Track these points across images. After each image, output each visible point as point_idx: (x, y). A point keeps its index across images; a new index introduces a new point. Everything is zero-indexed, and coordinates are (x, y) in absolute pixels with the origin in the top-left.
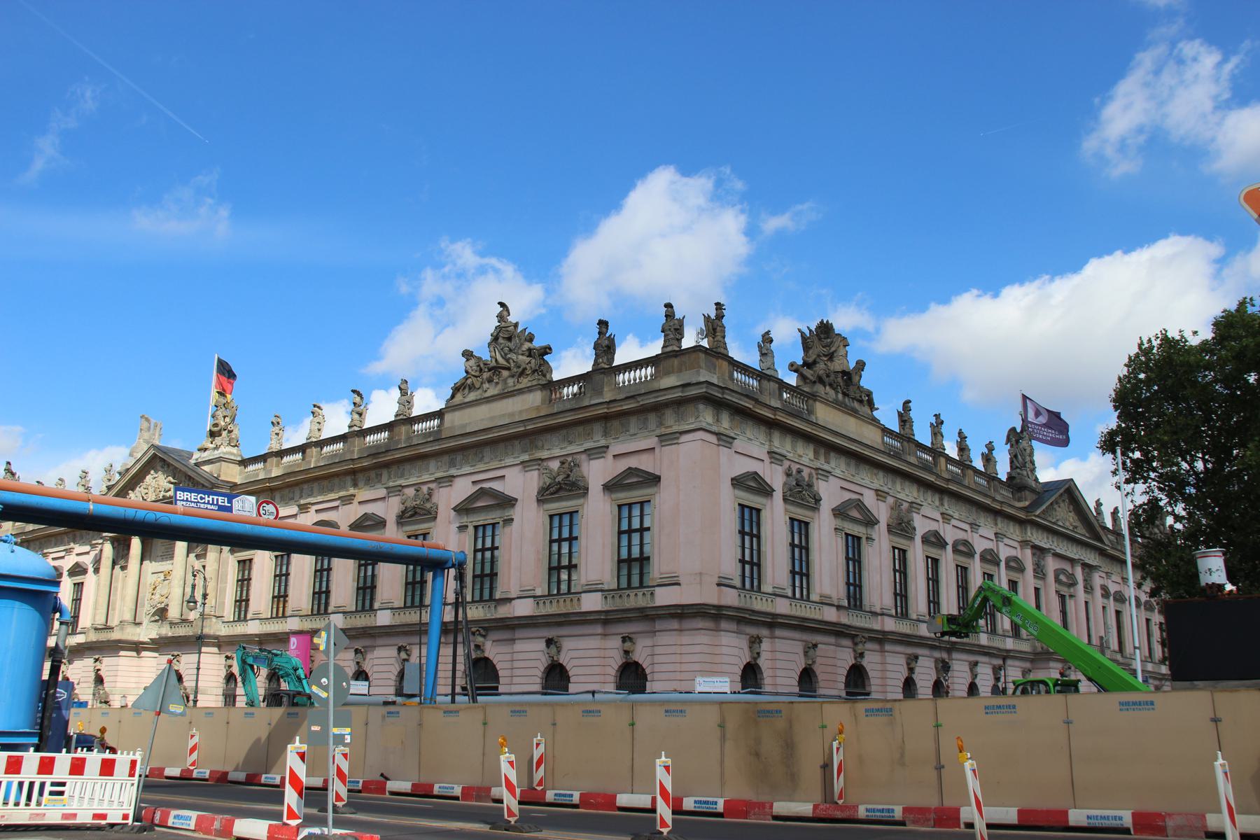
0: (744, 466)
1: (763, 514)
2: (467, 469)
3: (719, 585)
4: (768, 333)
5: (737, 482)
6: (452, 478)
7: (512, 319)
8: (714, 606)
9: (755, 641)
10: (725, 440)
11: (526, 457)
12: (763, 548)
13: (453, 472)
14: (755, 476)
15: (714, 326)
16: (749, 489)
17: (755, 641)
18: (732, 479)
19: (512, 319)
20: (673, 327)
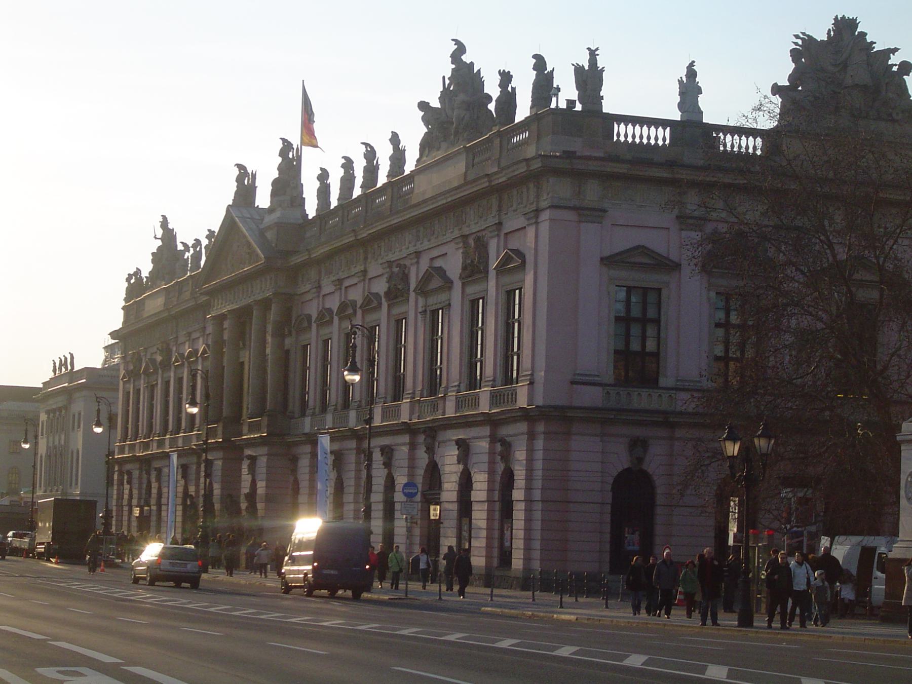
0: (622, 241)
1: (664, 292)
2: (426, 245)
3: (573, 383)
4: (693, 62)
5: (608, 261)
6: (418, 254)
7: (466, 58)
8: (555, 408)
9: (638, 445)
10: (592, 214)
11: (456, 233)
12: (662, 335)
13: (420, 247)
14: (642, 250)
15: (590, 79)
16: (641, 266)
17: (638, 445)
18: (602, 259)
19: (466, 58)
20: (544, 85)
